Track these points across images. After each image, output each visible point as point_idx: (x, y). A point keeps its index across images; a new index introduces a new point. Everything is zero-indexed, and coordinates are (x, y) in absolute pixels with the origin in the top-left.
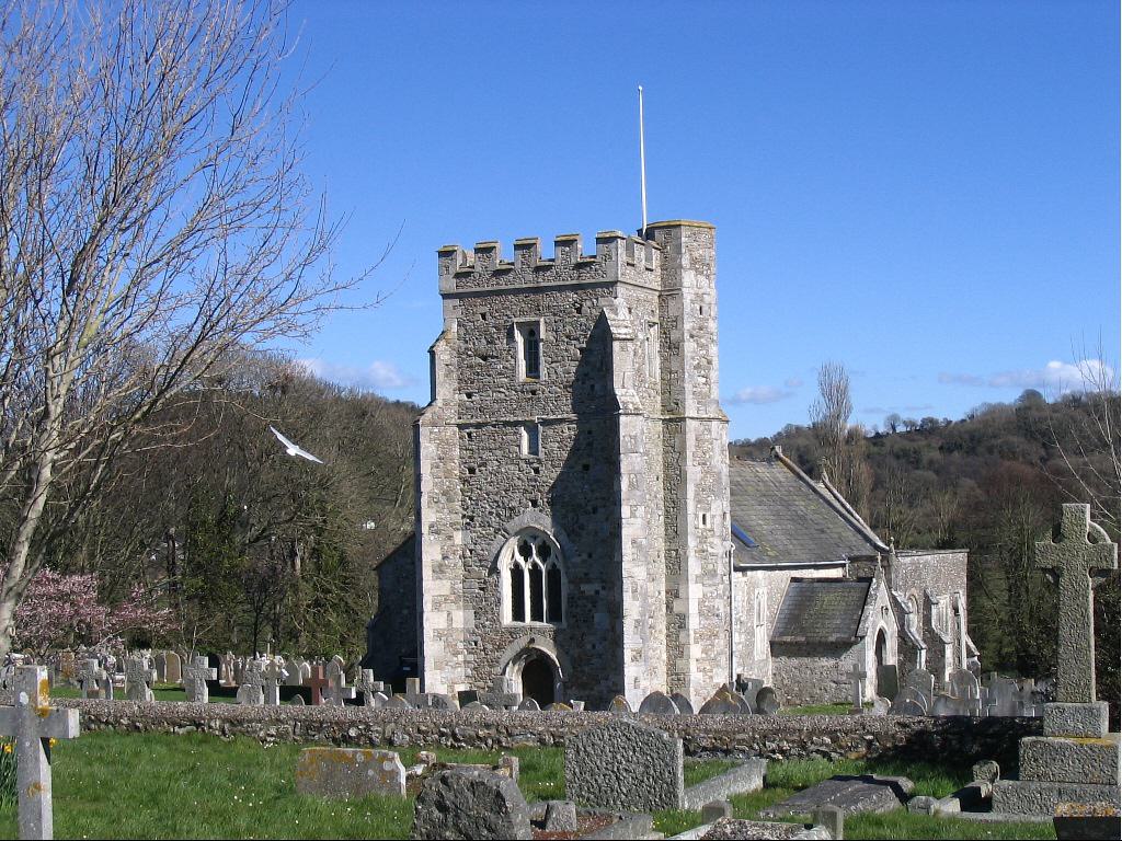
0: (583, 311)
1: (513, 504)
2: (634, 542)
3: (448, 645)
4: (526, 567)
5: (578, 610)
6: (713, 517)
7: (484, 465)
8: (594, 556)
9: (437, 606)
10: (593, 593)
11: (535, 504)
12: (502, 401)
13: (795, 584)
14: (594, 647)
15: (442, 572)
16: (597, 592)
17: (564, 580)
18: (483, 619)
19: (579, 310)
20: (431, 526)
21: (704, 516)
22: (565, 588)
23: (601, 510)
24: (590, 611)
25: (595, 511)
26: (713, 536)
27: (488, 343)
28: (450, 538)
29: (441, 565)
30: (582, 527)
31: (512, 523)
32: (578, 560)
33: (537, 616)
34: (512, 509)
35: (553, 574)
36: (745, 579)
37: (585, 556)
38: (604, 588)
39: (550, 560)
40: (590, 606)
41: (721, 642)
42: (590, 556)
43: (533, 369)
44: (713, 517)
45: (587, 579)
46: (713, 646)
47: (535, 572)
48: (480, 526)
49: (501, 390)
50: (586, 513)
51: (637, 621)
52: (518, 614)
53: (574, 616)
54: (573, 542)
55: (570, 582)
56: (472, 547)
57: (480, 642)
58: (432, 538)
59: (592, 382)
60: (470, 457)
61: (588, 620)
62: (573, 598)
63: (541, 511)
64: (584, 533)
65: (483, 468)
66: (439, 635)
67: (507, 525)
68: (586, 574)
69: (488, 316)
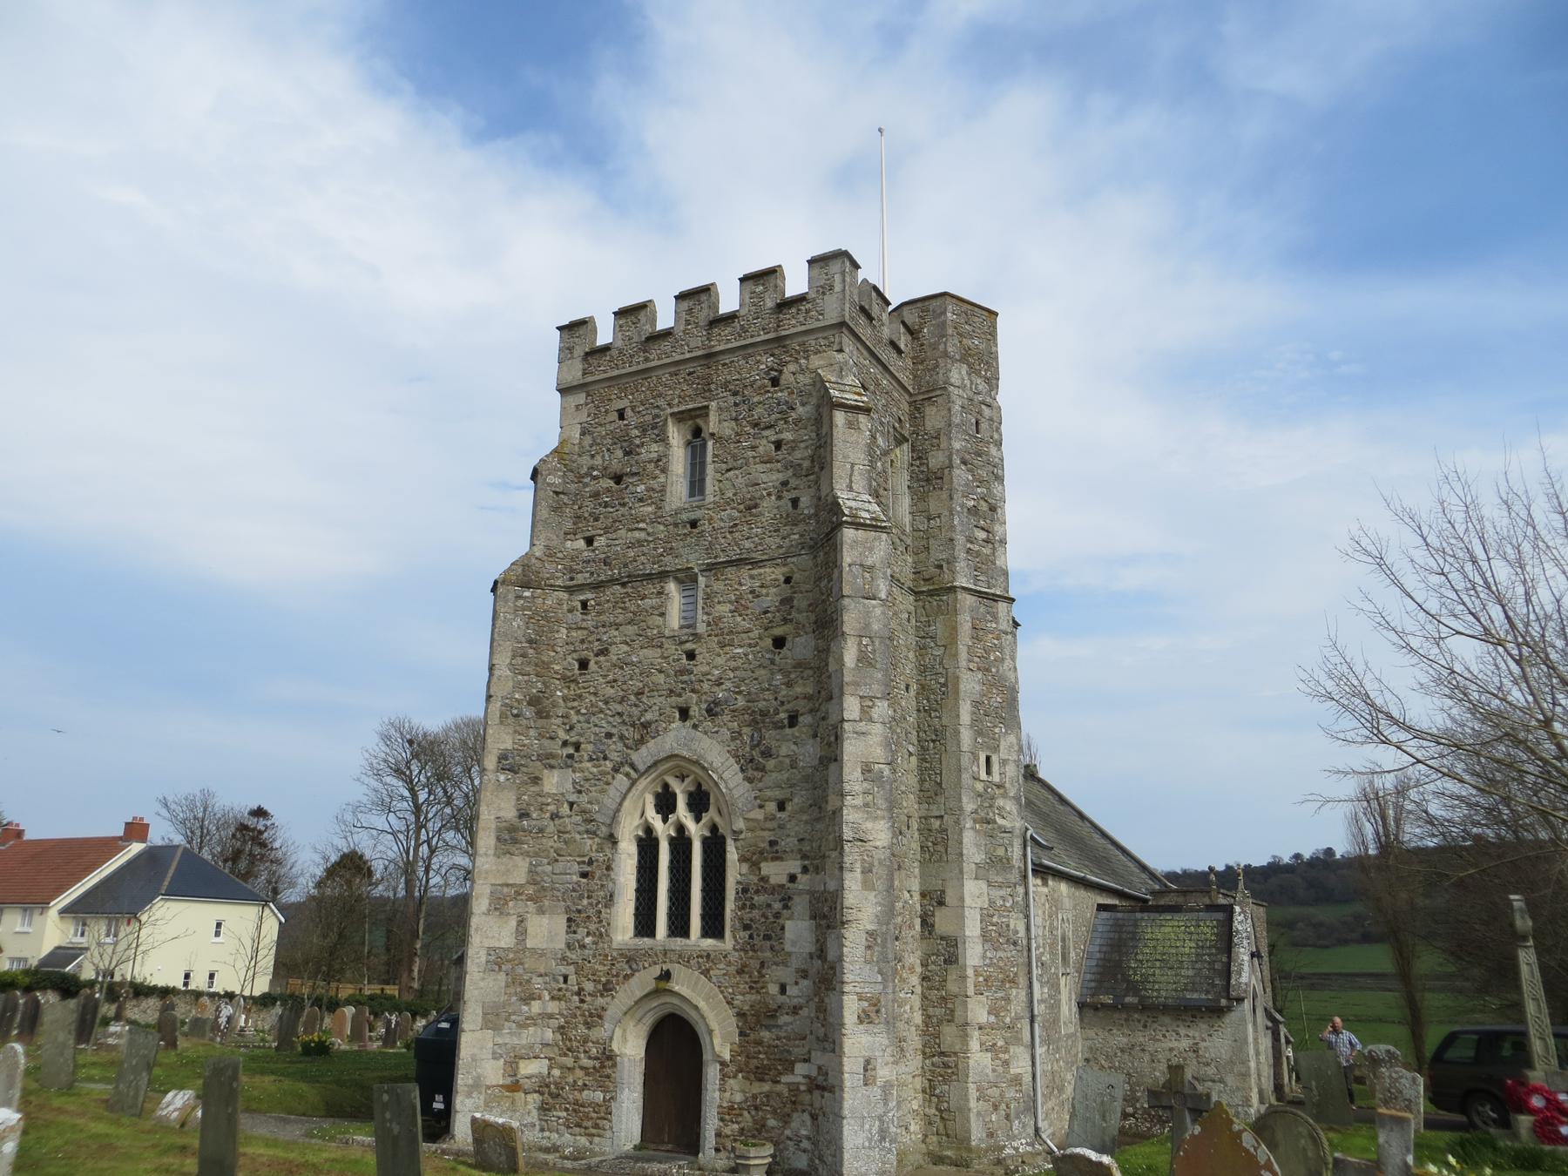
0: (782, 382)
1: (648, 716)
2: (867, 770)
3: (514, 980)
4: (663, 831)
5: (756, 913)
6: (1004, 763)
7: (604, 652)
8: (789, 807)
9: (499, 906)
10: (783, 880)
11: (684, 714)
12: (640, 543)
13: (1105, 915)
14: (783, 989)
15: (515, 841)
16: (793, 878)
17: (732, 854)
18: (582, 931)
19: (775, 382)
20: (503, 757)
21: (988, 759)
22: (735, 872)
23: (805, 720)
24: (777, 915)
25: (793, 720)
26: (1005, 796)
27: (627, 453)
28: (536, 780)
29: (512, 829)
30: (767, 754)
31: (643, 750)
32: (758, 814)
33: (679, 926)
34: (646, 726)
35: (715, 846)
36: (1045, 890)
37: (772, 807)
38: (805, 870)
39: (706, 818)
40: (777, 906)
41: (1018, 995)
42: (781, 806)
43: (696, 485)
44: (1004, 763)
45: (774, 852)
46: (1007, 999)
47: (681, 844)
48: (591, 759)
49: (642, 525)
50: (779, 726)
51: (870, 934)
52: (645, 925)
53: (746, 927)
54: (750, 780)
55: (742, 859)
56: (573, 798)
57: (572, 979)
58: (502, 778)
59: (794, 494)
60: (582, 641)
61: (773, 934)
62: (745, 891)
63: (695, 727)
64: (771, 764)
65: (602, 658)
66: (498, 960)
67: (635, 757)
68: (772, 843)
69: (629, 413)
